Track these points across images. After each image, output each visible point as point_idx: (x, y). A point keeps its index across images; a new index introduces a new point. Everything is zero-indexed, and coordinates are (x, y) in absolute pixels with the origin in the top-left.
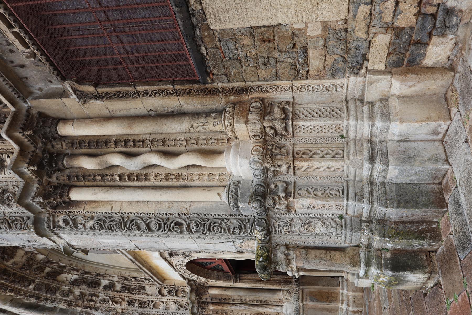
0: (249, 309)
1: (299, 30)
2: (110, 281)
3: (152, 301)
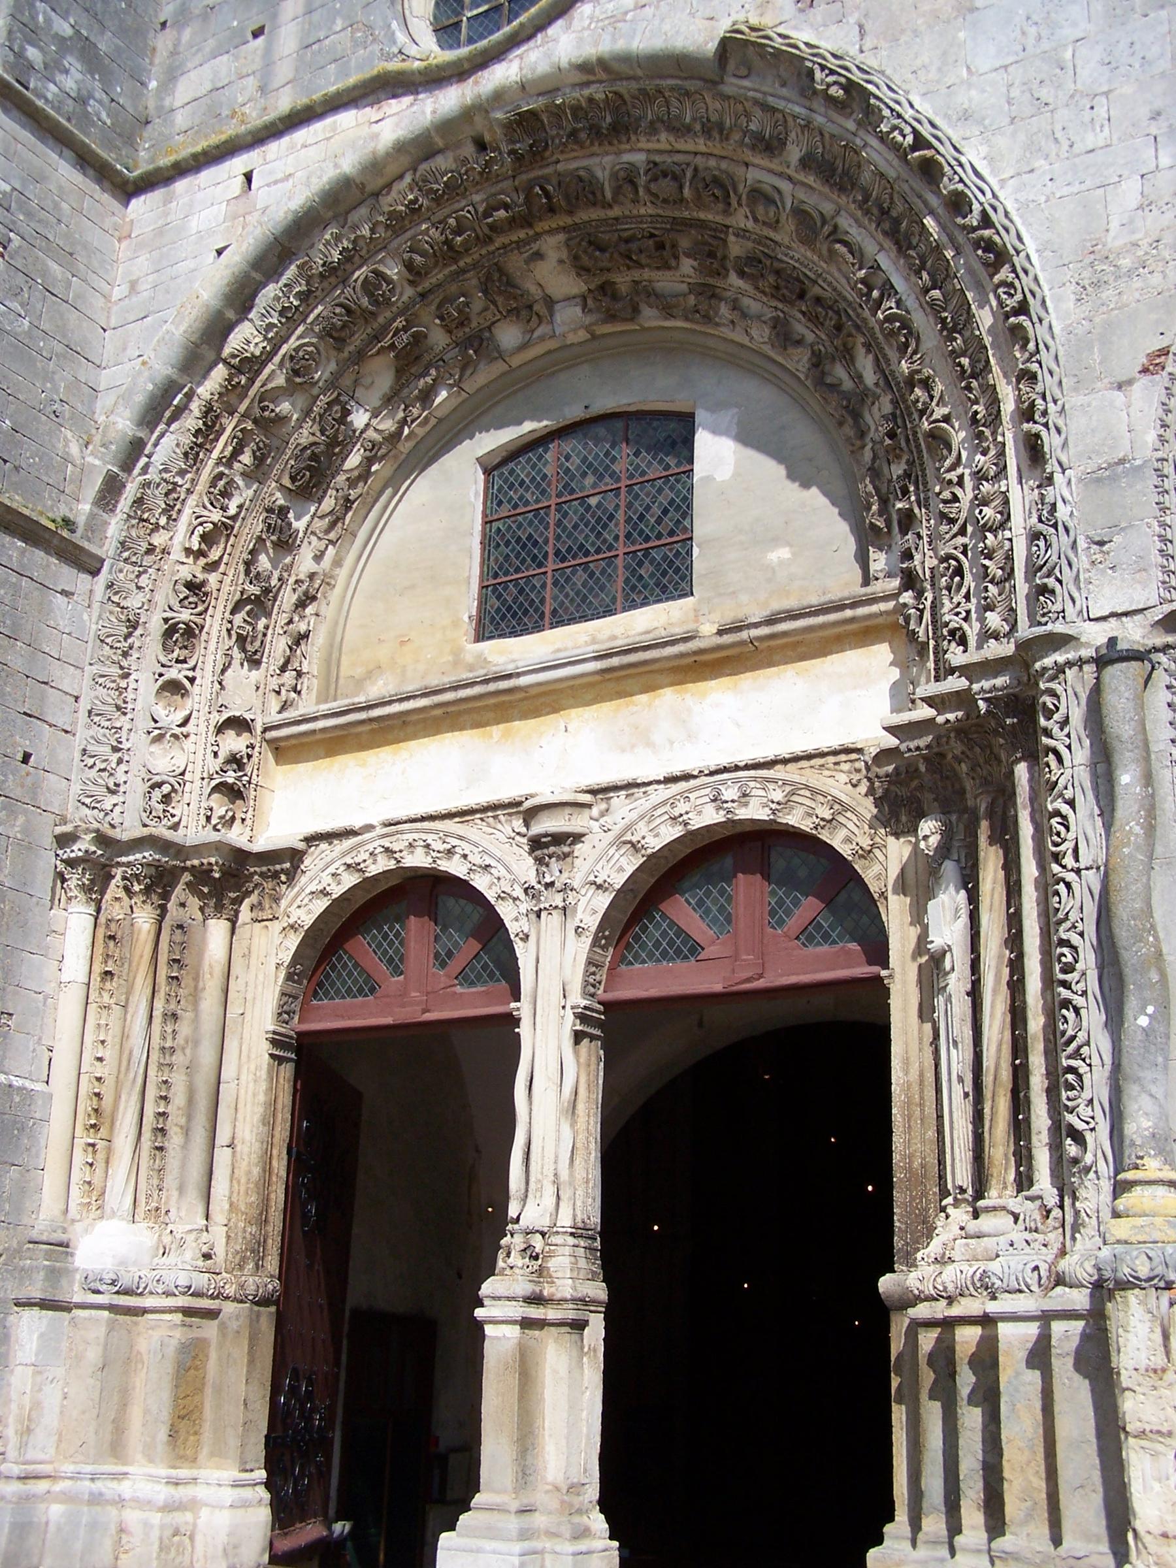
0: (132, 1075)
2: (301, 535)
3: (192, 680)
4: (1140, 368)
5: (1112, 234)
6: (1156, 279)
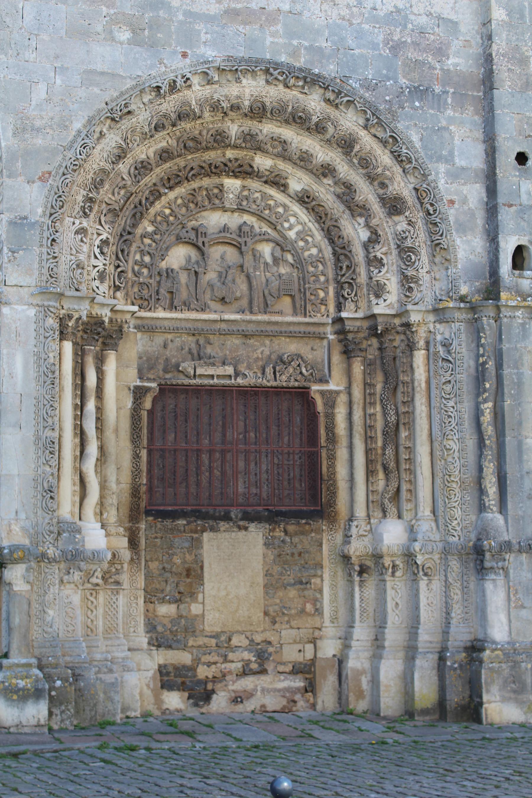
1: (197, 598)
4: (37, 177)
5: (32, 107)
6: (49, 137)
